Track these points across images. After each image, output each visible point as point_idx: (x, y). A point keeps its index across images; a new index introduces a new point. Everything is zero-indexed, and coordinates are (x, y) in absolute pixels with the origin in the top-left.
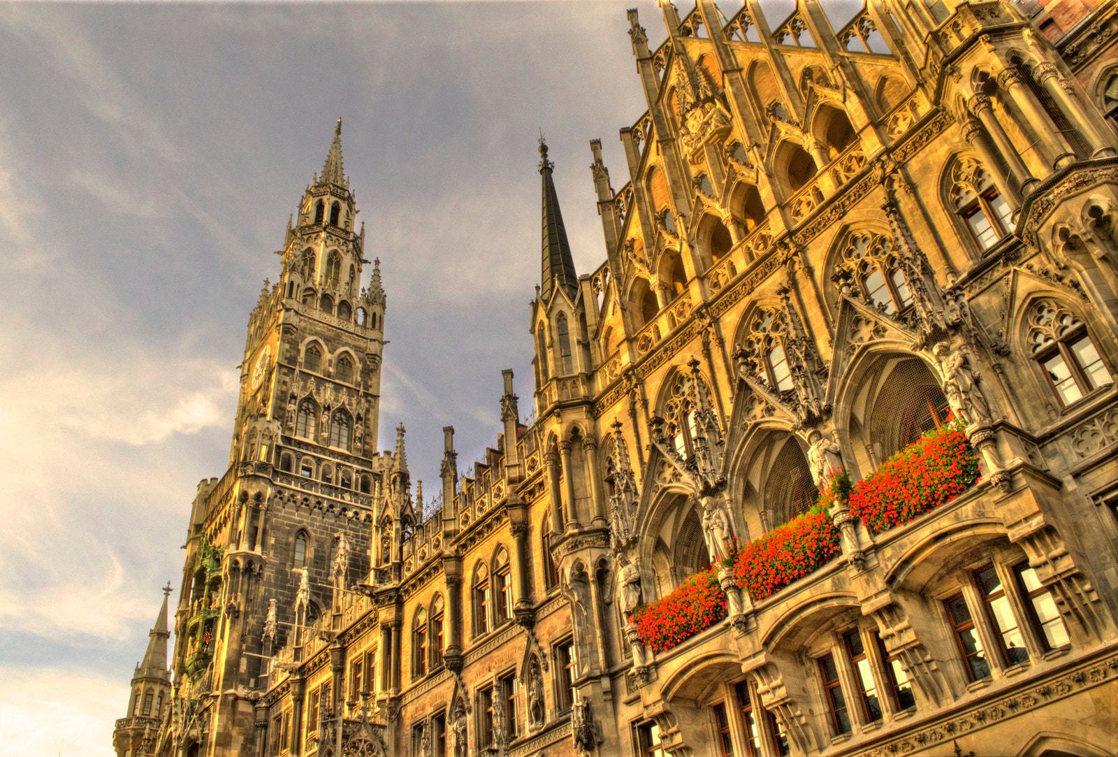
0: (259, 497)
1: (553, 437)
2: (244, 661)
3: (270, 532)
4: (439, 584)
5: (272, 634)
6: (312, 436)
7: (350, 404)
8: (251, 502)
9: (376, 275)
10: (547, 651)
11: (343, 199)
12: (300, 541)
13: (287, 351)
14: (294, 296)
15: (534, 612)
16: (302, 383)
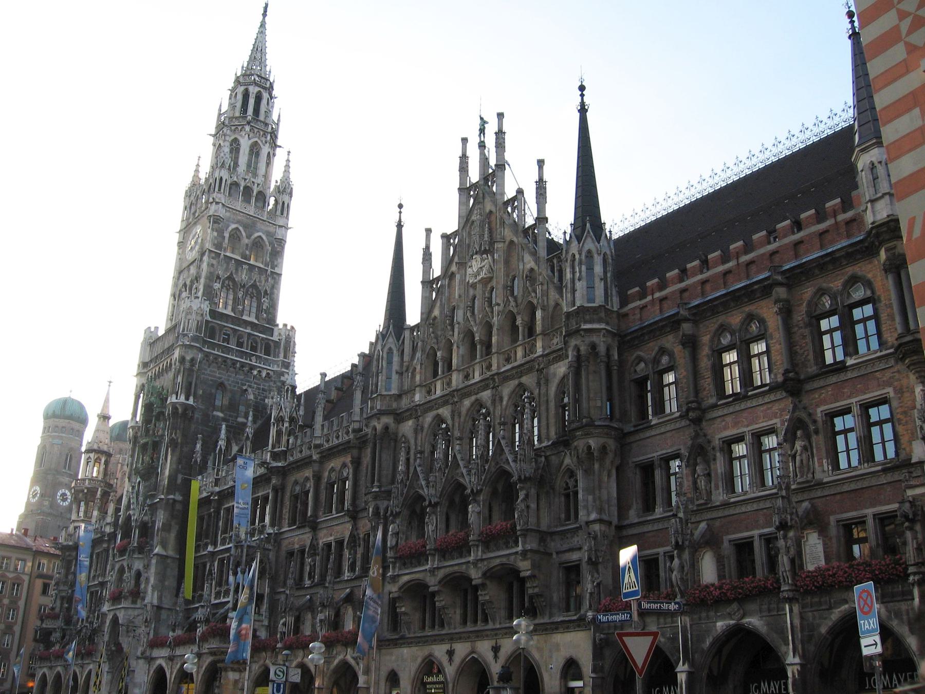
0: (192, 360)
4: (308, 473)
5: (199, 460)
6: (230, 308)
7: (260, 282)
8: (188, 365)
12: (219, 391)
13: (215, 238)
15: (357, 512)
16: (225, 266)
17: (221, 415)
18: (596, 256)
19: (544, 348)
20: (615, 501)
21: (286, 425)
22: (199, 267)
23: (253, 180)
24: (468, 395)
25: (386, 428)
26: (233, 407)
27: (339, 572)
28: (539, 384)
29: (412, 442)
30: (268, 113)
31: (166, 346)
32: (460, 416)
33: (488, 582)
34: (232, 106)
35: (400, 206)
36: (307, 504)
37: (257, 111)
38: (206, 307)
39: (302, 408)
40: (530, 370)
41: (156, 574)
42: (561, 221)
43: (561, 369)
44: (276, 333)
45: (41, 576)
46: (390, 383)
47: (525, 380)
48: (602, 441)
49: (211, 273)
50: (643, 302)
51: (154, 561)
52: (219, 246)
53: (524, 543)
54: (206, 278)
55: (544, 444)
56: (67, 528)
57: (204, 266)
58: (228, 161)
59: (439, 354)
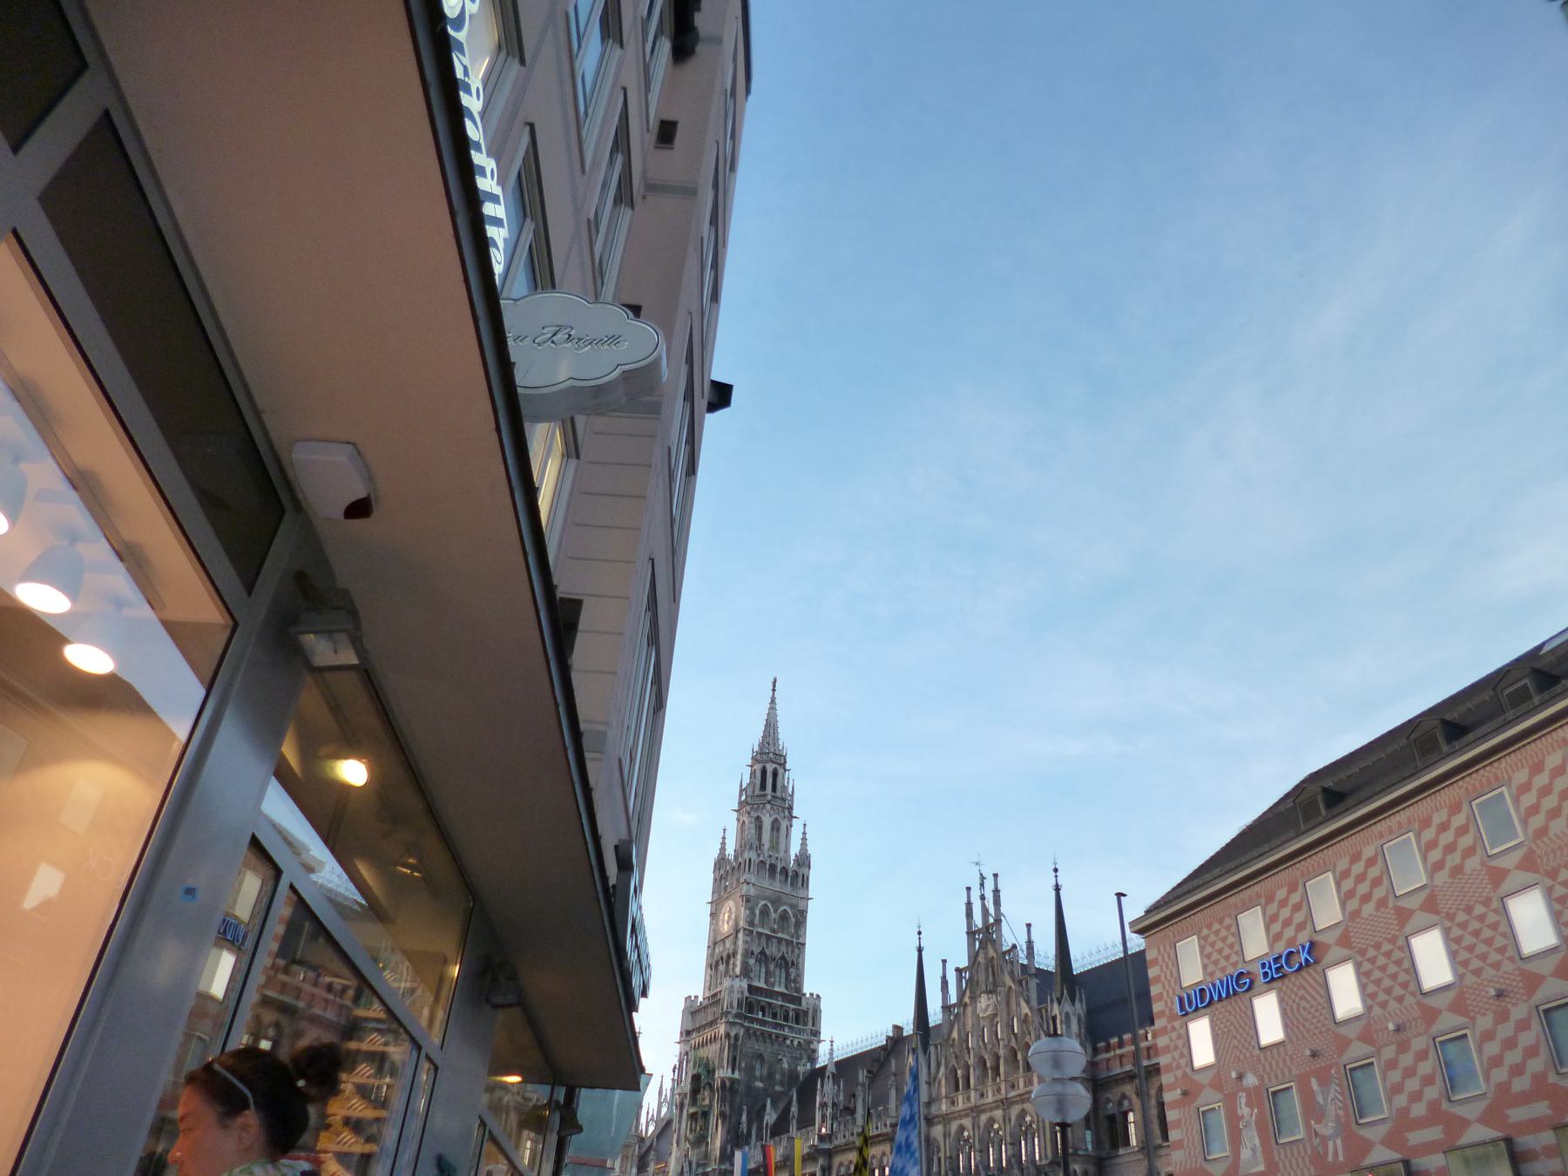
0: (736, 1036)
9: (804, 839)
22: (735, 943)
26: (771, 1076)
30: (785, 788)
31: (710, 1019)
34: (752, 783)
42: (1046, 957)
44: (804, 1002)
52: (751, 923)
57: (740, 942)
59: (959, 1072)
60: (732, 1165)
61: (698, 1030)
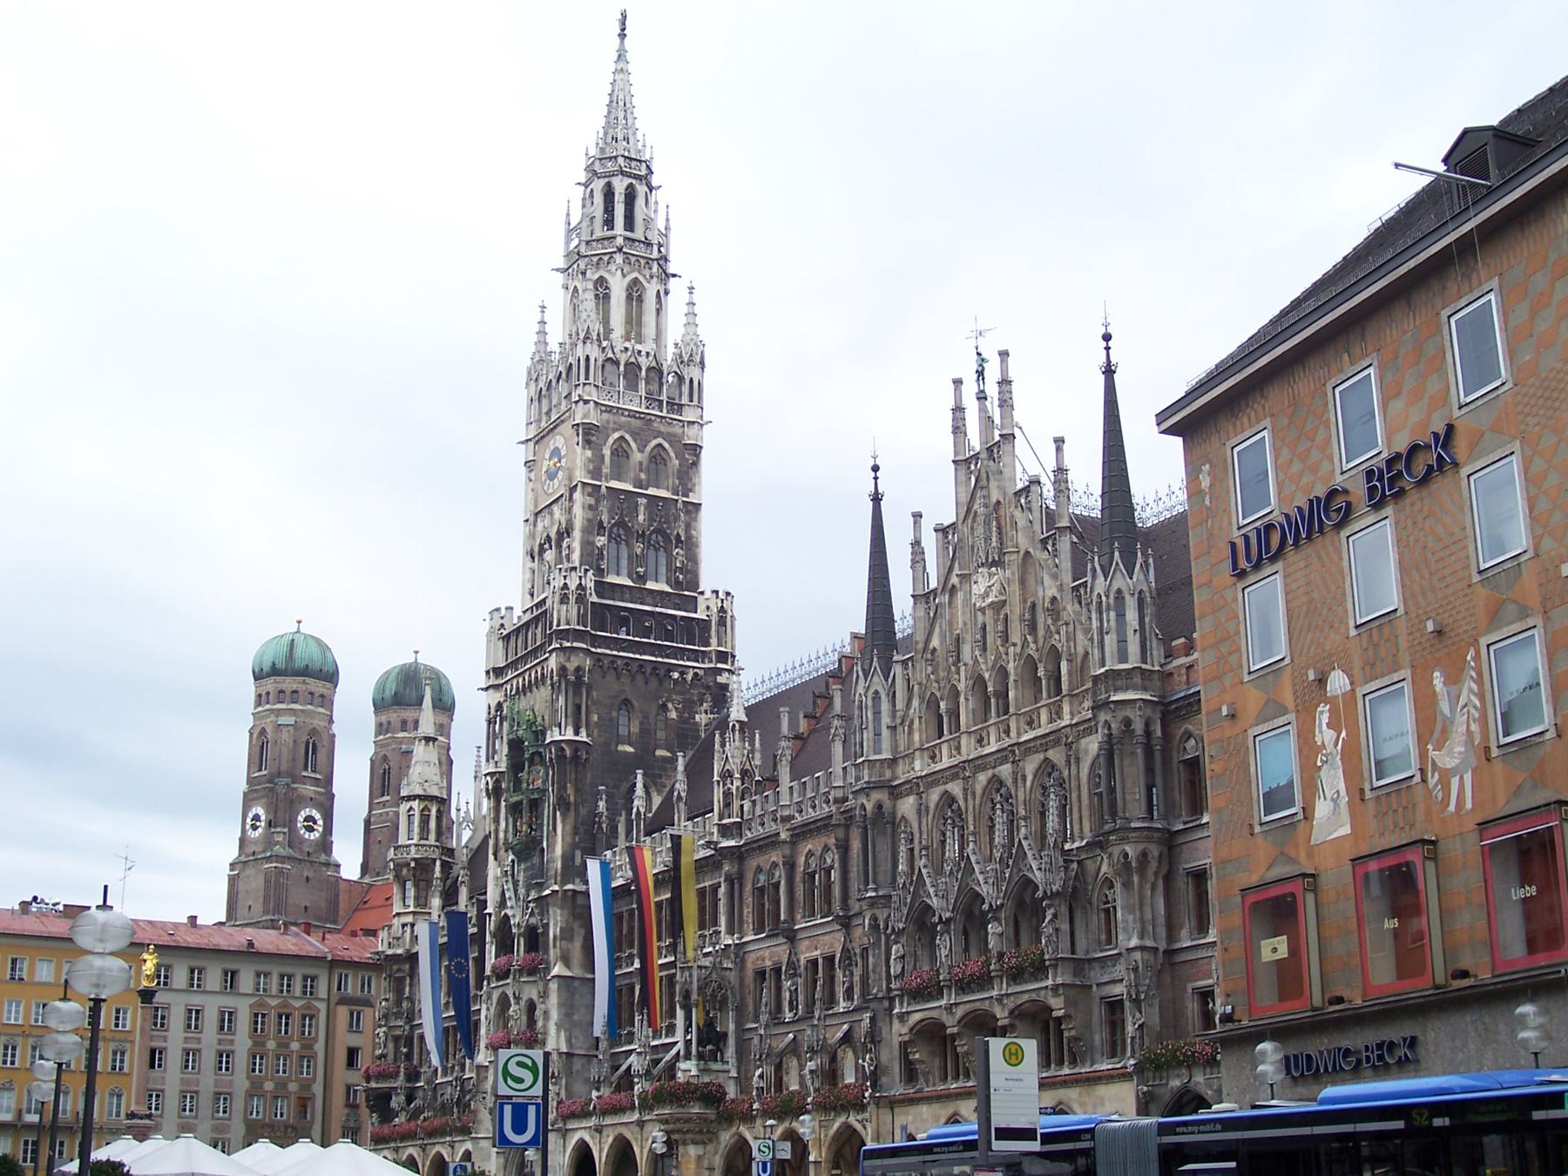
0: (578, 669)
1: (863, 807)
2: (578, 853)
3: (593, 708)
4: (775, 856)
6: (624, 571)
10: (858, 951)
11: (638, 178)
13: (590, 460)
14: (591, 380)
15: (850, 918)
17: (631, 750)
18: (1127, 597)
19: (1072, 714)
20: (1161, 920)
21: (737, 783)
23: (638, 347)
24: (984, 768)
25: (879, 806)
27: (831, 1001)
28: (1068, 763)
29: (915, 826)
30: (647, 222)
32: (974, 794)
33: (1017, 1022)
35: (875, 469)
36: (778, 901)
37: (630, 223)
38: (589, 582)
39: (758, 755)
40: (1057, 743)
41: (560, 1005)
43: (1092, 745)
44: (701, 606)
45: (344, 1001)
46: (880, 741)
47: (1051, 754)
48: (1141, 847)
49: (589, 520)
50: (1190, 659)
51: (553, 986)
52: (596, 473)
53: (1055, 976)
54: (585, 531)
55: (1076, 845)
56: (390, 927)
58: (597, 327)
59: (943, 705)
60: (586, 883)
61: (512, 665)
